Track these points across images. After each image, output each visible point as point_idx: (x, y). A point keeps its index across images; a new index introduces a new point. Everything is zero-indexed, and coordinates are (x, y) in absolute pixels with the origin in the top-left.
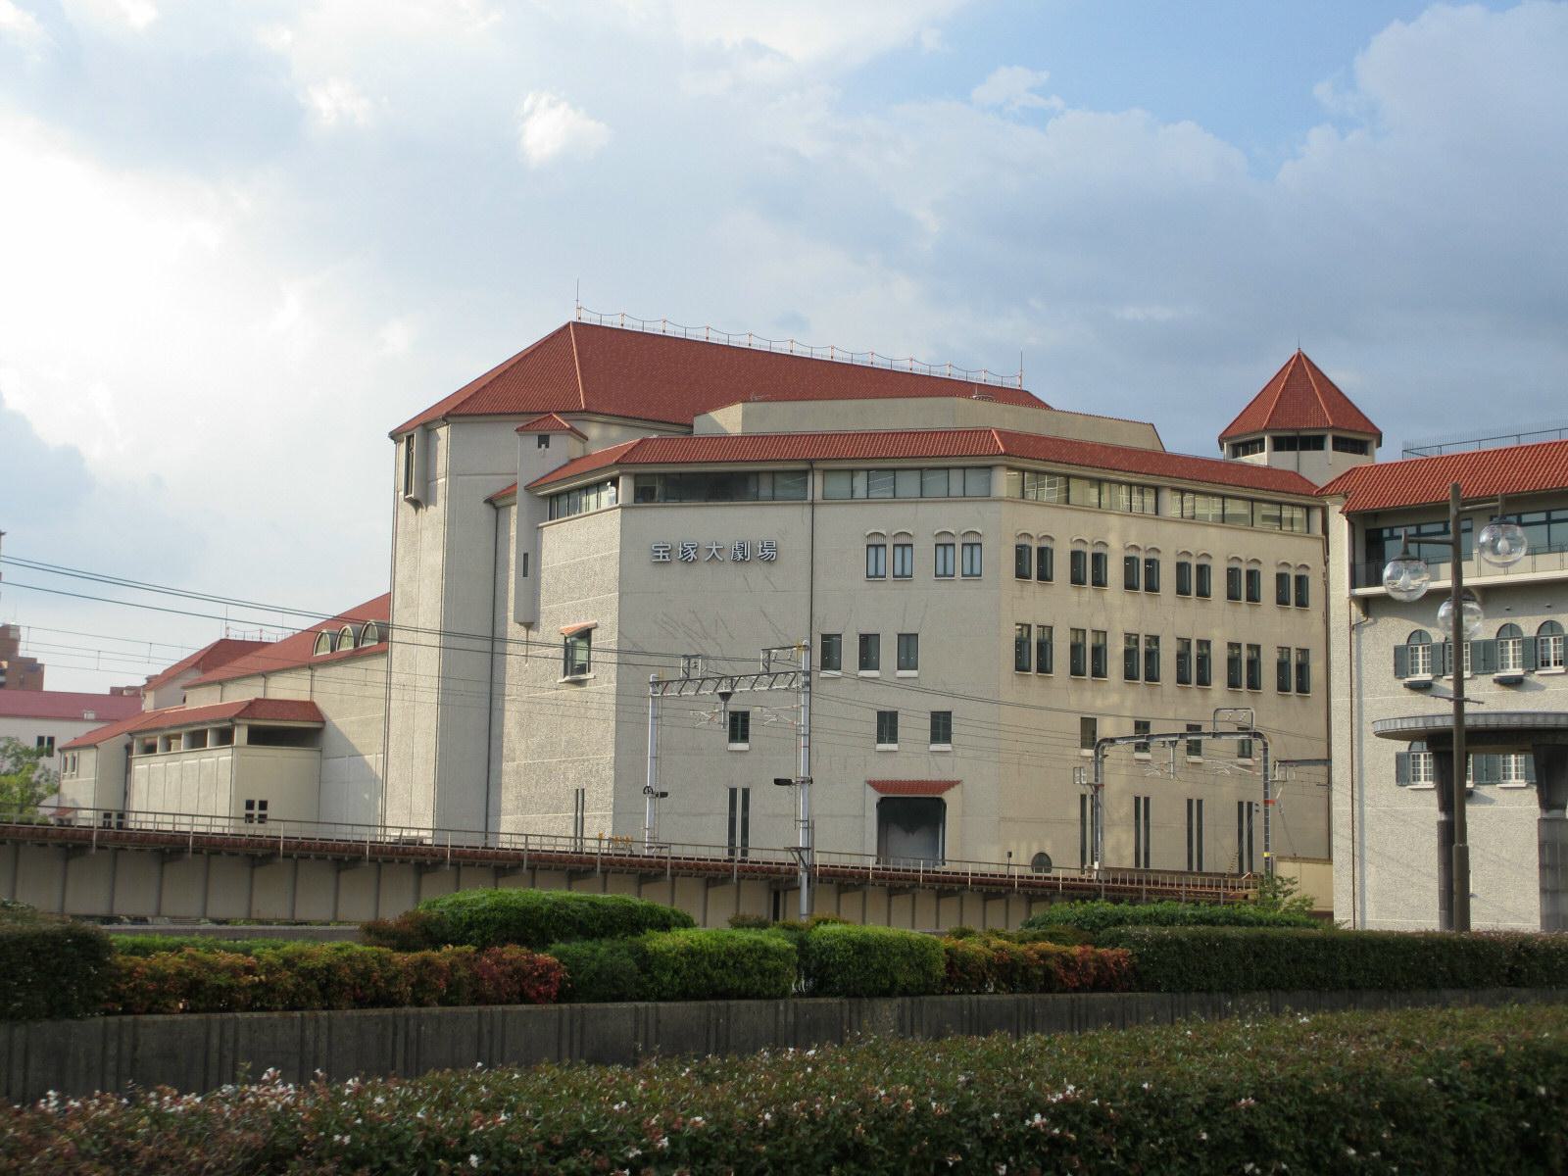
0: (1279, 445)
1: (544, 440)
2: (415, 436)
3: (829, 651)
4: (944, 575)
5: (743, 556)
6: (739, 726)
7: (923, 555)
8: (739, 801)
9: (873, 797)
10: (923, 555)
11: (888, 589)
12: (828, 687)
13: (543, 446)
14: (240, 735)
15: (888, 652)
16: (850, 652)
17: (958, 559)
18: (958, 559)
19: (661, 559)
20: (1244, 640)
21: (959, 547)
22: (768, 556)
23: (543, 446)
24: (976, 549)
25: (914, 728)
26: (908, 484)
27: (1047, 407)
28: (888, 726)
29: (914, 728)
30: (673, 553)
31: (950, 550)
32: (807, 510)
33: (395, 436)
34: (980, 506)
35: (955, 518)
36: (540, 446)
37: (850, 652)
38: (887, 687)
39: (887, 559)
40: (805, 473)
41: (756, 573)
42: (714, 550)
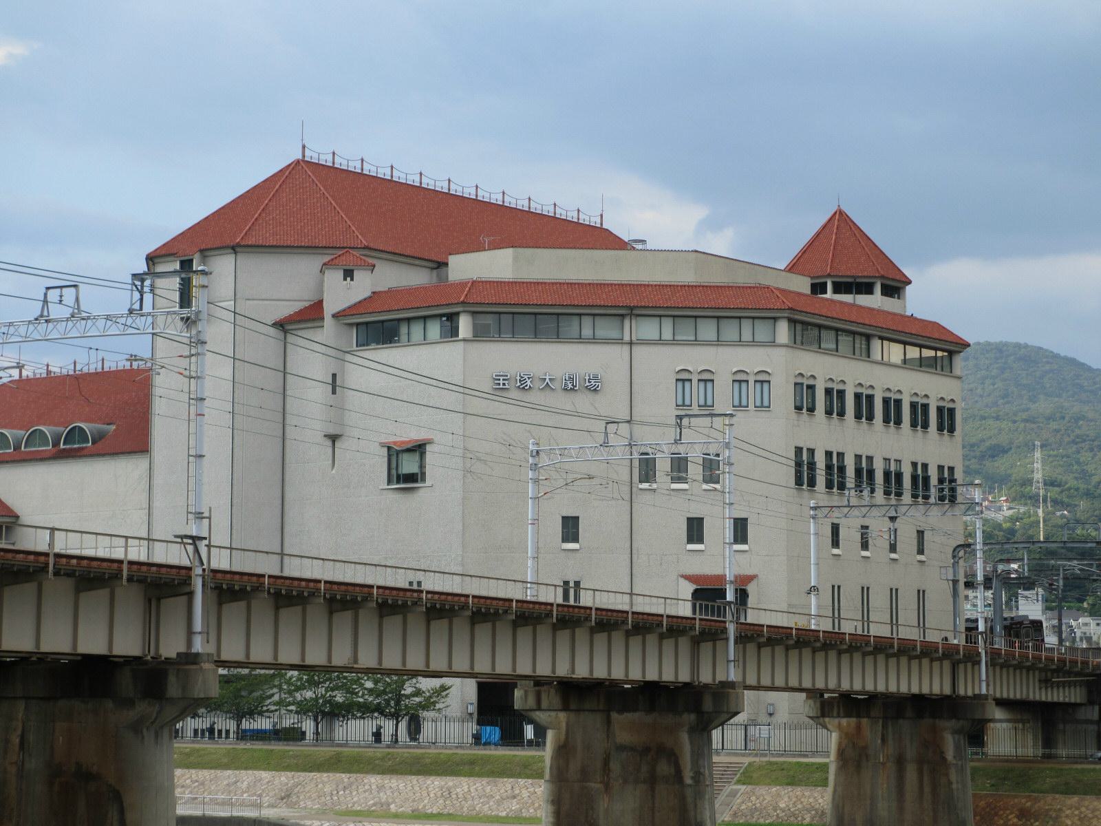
1: (349, 274)
3: (647, 470)
5: (570, 387)
6: (570, 529)
12: (648, 497)
13: (349, 279)
19: (501, 386)
21: (751, 383)
23: (349, 279)
24: (766, 386)
25: (718, 529)
26: (707, 330)
28: (695, 530)
29: (718, 529)
30: (513, 383)
31: (744, 385)
32: (626, 348)
34: (769, 350)
35: (751, 360)
36: (345, 279)
39: (696, 393)
40: (623, 316)
42: (547, 380)
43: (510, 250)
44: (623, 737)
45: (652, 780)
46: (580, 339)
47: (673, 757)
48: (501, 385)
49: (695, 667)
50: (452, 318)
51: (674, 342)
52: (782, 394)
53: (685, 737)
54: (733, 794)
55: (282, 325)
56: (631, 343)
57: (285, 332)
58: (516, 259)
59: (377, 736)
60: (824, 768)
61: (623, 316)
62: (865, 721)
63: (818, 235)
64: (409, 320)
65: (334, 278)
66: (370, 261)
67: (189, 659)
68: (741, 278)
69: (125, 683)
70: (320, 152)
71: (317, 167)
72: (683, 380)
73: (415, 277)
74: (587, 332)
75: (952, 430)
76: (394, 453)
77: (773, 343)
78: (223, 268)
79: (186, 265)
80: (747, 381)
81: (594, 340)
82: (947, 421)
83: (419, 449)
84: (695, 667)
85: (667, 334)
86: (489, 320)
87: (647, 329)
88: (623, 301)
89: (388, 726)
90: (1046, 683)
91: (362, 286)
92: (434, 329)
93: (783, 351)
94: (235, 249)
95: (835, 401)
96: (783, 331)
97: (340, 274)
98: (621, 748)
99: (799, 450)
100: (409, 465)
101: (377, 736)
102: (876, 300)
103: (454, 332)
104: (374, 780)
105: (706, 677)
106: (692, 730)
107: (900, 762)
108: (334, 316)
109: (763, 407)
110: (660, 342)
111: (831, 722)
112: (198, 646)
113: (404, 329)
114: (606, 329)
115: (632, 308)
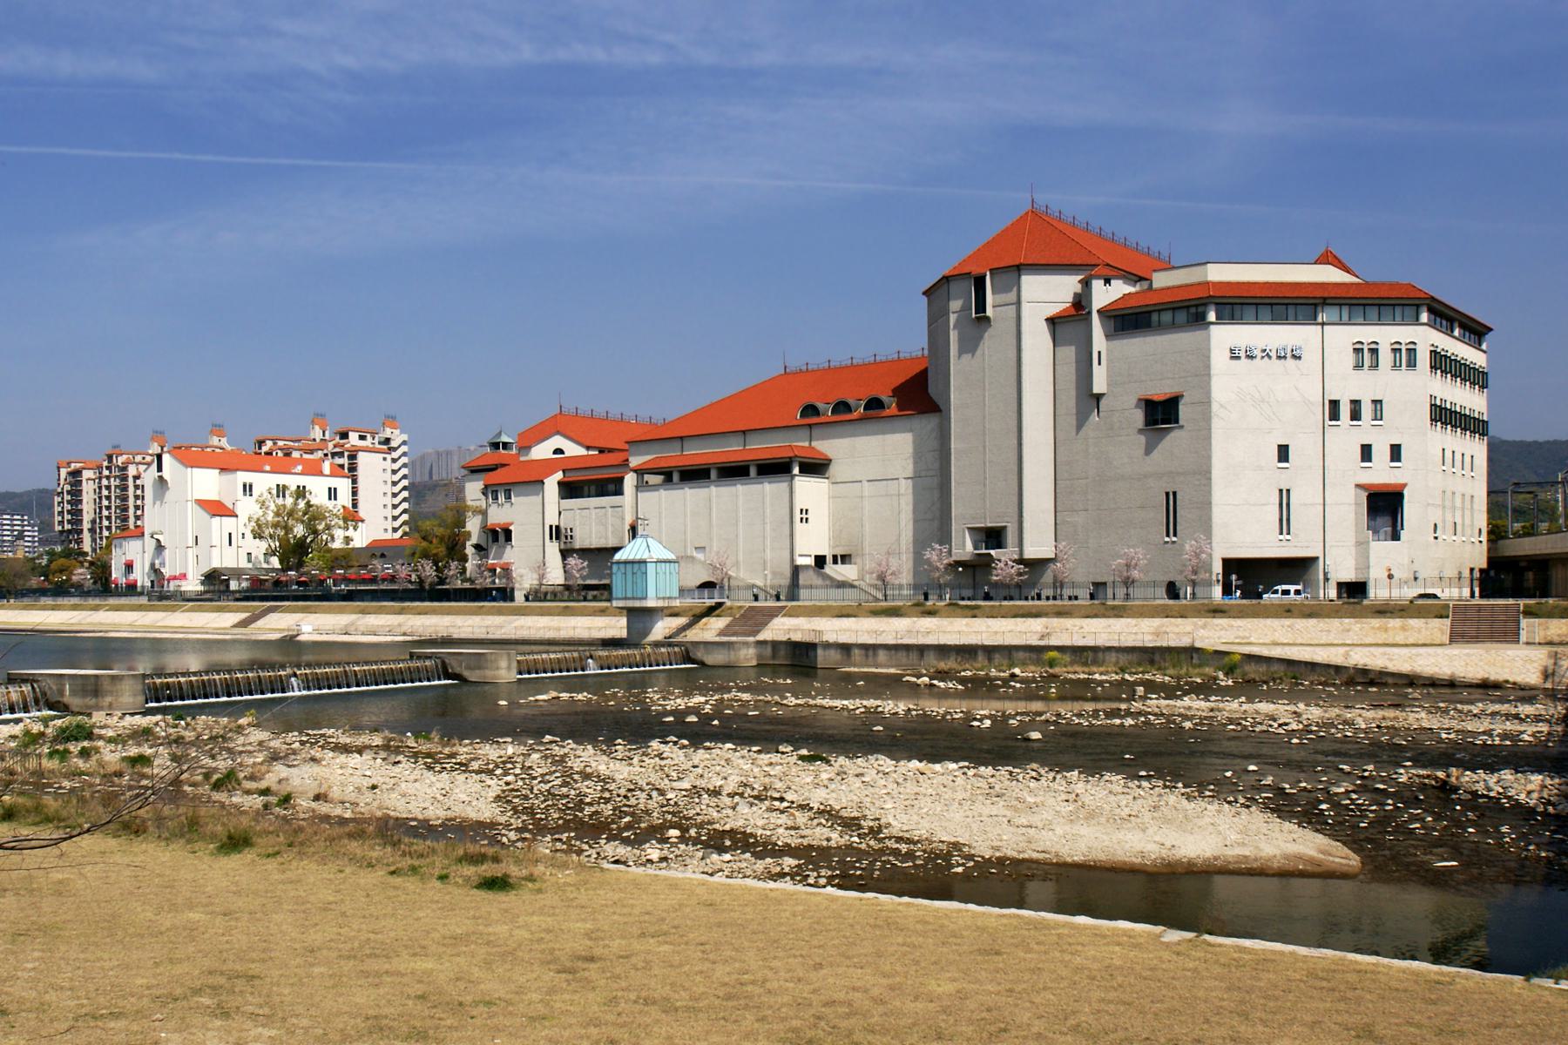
6: (1283, 453)
7: (1385, 357)
10: (1385, 357)
16: (1345, 411)
21: (1404, 352)
25: (1381, 453)
28: (1366, 452)
29: (1381, 453)
35: (1403, 334)
37: (1345, 411)
38: (1366, 431)
58: (1206, 276)
80: (1400, 350)
85: (1345, 317)
97: (1102, 282)
108: (1098, 311)
115: (1325, 299)
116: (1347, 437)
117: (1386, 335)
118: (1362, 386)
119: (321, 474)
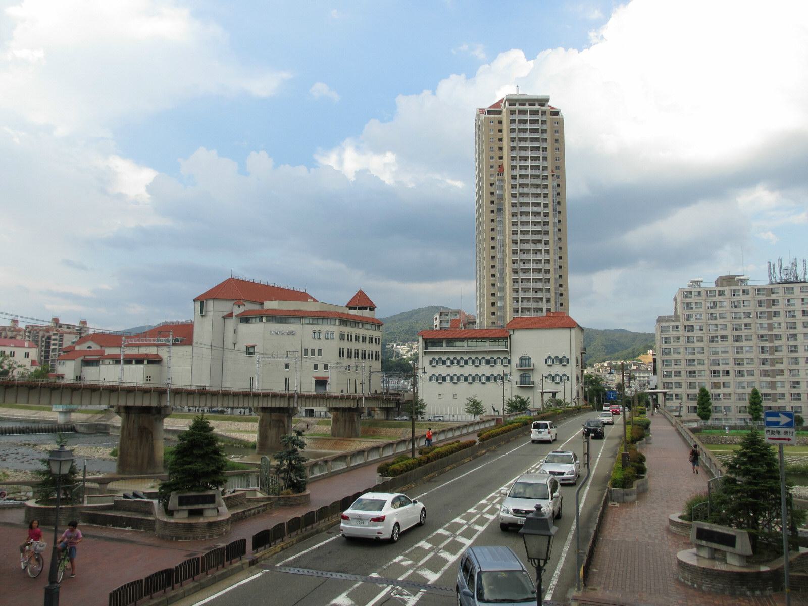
0: (359, 308)
2: (202, 300)
4: (327, 339)
7: (323, 335)
8: (287, 380)
9: (314, 380)
10: (323, 335)
11: (317, 341)
14: (146, 362)
15: (316, 352)
16: (309, 352)
17: (330, 336)
18: (330, 336)
20: (371, 350)
22: (293, 334)
25: (321, 366)
26: (320, 321)
27: (318, 302)
28: (316, 366)
29: (321, 366)
33: (195, 301)
35: (330, 328)
37: (309, 352)
39: (317, 335)
41: (291, 337)
43: (277, 302)
44: (273, 418)
45: (279, 427)
46: (291, 323)
47: (283, 422)
48: (272, 333)
49: (289, 404)
50: (262, 318)
51: (313, 324)
52: (337, 336)
53: (286, 419)
54: (314, 427)
55: (224, 317)
56: (302, 324)
57: (224, 319)
59: (241, 413)
60: (330, 421)
61: (301, 318)
62: (338, 412)
63: (355, 296)
64: (252, 317)
65: (236, 307)
66: (245, 303)
67: (166, 406)
68: (331, 309)
69: (154, 411)
70: (235, 276)
71: (234, 280)
72: (314, 333)
73: (256, 307)
74: (293, 321)
75: (379, 343)
76: (248, 348)
77: (335, 325)
78: (210, 305)
79: (202, 303)
81: (294, 323)
82: (377, 341)
83: (253, 347)
84: (289, 404)
85: (311, 322)
86: (270, 318)
87: (307, 321)
88: (301, 315)
89: (243, 410)
90: (383, 403)
91: (242, 309)
92: (258, 320)
93: (337, 326)
94: (213, 299)
95: (350, 338)
96: (337, 322)
98: (273, 420)
99: (340, 349)
100: (251, 350)
101: (241, 413)
102: (367, 313)
103: (262, 321)
104: (237, 423)
105: (291, 406)
106: (287, 417)
107: (345, 421)
108: (236, 316)
109: (332, 339)
110: (309, 324)
111: (332, 413)
112: (168, 404)
113: (251, 320)
114: (297, 321)
116: (309, 362)
117: (324, 328)
118: (316, 345)
119: (24, 347)
